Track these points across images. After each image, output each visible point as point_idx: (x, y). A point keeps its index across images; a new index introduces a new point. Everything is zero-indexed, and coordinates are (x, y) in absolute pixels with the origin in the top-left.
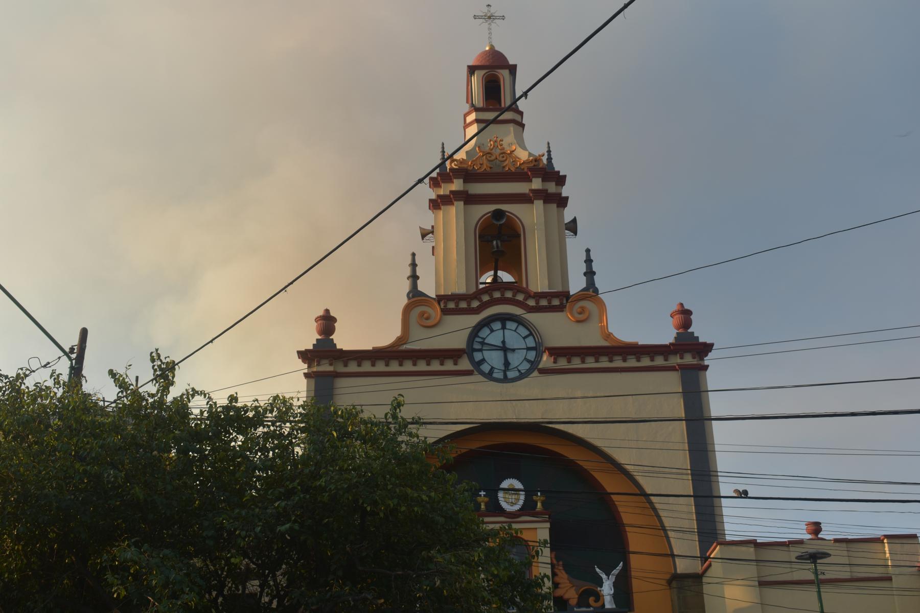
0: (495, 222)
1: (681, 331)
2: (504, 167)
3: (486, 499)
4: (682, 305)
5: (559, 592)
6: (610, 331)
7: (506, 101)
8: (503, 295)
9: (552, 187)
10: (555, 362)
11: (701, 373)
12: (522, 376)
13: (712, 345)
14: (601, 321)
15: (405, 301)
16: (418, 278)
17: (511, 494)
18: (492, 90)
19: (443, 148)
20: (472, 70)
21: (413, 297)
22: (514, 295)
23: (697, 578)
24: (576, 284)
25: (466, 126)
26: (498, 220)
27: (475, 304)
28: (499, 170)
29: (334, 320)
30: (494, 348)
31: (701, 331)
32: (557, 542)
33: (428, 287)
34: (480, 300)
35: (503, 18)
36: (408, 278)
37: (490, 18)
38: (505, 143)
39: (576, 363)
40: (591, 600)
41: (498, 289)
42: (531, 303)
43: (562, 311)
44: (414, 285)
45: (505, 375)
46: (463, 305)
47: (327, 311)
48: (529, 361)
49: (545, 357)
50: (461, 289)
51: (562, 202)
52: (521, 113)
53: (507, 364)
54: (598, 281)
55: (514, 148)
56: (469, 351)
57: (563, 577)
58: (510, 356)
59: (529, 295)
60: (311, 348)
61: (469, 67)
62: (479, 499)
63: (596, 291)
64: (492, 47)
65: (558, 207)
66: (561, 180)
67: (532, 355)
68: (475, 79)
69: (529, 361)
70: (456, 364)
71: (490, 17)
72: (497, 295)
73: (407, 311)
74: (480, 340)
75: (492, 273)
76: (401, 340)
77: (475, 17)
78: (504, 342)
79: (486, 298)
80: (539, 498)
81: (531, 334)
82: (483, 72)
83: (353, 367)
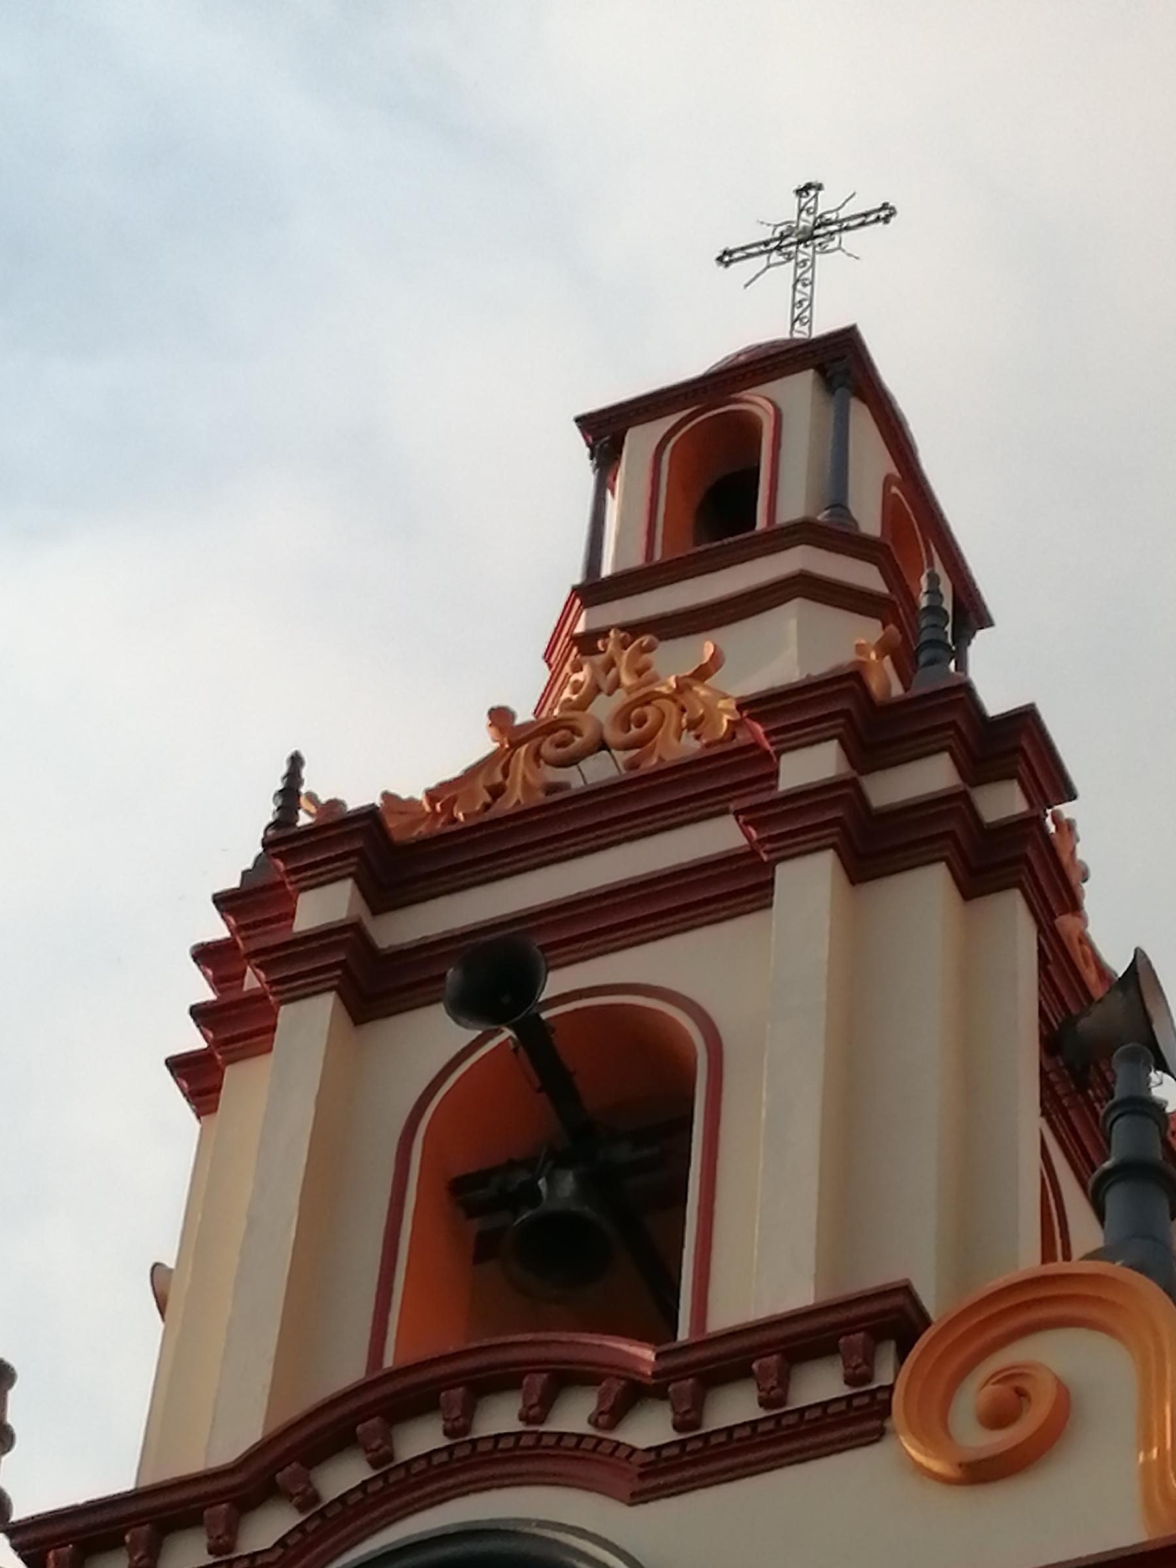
20: (605, 432)
34: (307, 1500)
35: (885, 214)
37: (807, 237)
42: (650, 1429)
43: (877, 1435)
61: (590, 424)
65: (974, 883)
72: (422, 1438)
79: (343, 1476)
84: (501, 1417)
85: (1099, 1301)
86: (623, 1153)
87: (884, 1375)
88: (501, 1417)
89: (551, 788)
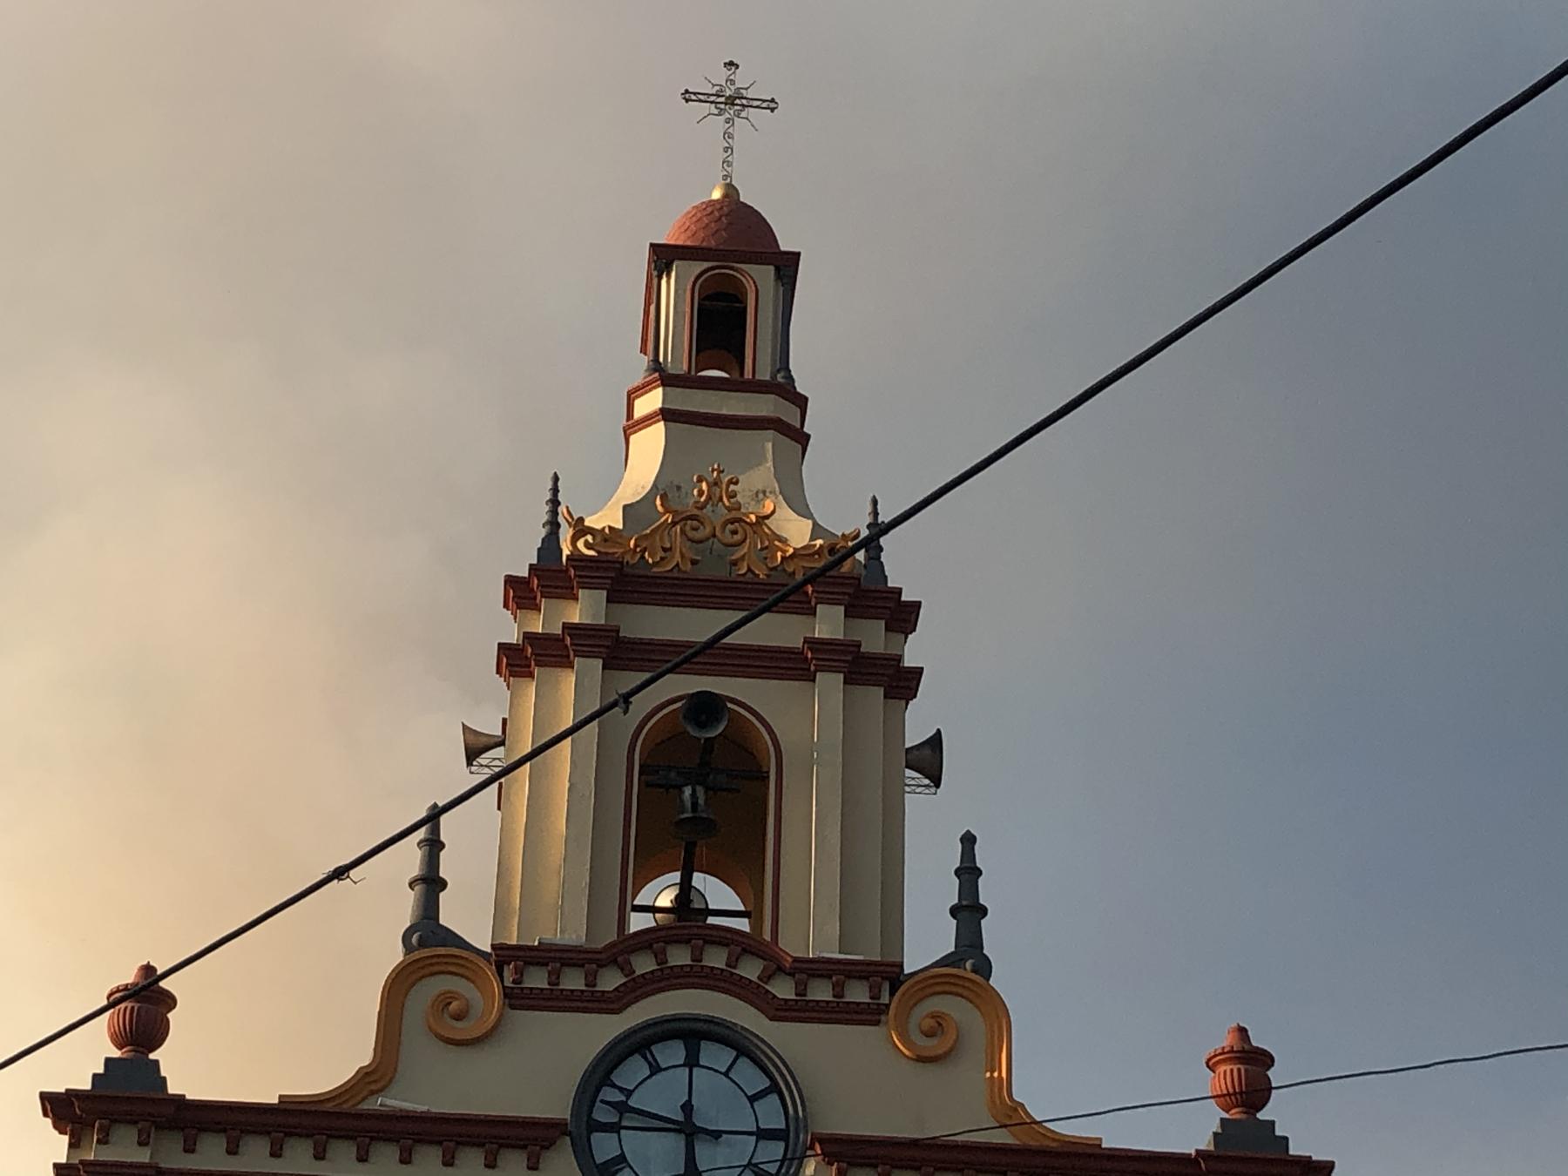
0: (692, 731)
1: (1235, 1114)
2: (734, 563)
4: (1242, 1032)
8: (697, 958)
9: (873, 637)
14: (993, 1065)
15: (397, 955)
16: (443, 884)
18: (720, 325)
19: (555, 490)
20: (663, 257)
21: (422, 944)
22: (733, 962)
24: (926, 940)
25: (633, 426)
26: (702, 726)
27: (611, 981)
28: (721, 572)
29: (169, 1001)
30: (656, 1123)
33: (470, 916)
34: (627, 969)
36: (411, 885)
37: (731, 101)
38: (743, 491)
42: (783, 989)
43: (877, 1023)
46: (573, 981)
50: (574, 934)
51: (904, 684)
52: (801, 402)
55: (769, 506)
56: (579, 1128)
59: (777, 965)
60: (86, 1085)
63: (984, 968)
64: (731, 191)
66: (903, 616)
68: (668, 288)
71: (732, 101)
72: (679, 957)
73: (398, 987)
75: (676, 877)
76: (367, 1080)
77: (687, 96)
78: (687, 1108)
79: (644, 964)
81: (774, 1088)
82: (698, 267)
84: (716, 959)
85: (978, 996)
87: (885, 999)
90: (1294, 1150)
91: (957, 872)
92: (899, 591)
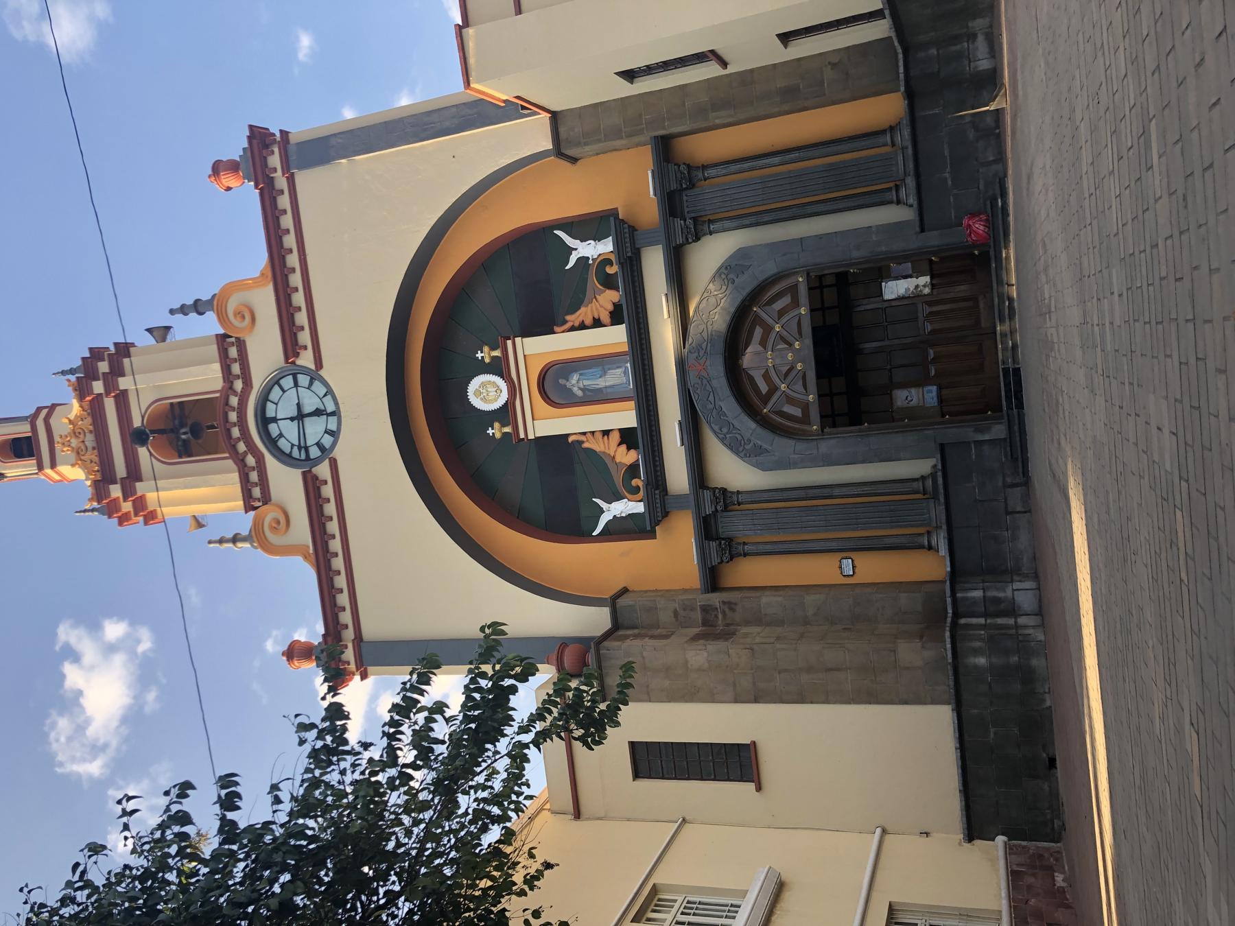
3: (497, 425)
5: (605, 318)
6: (258, 274)
7: (23, 430)
9: (103, 367)
10: (305, 348)
11: (293, 139)
12: (330, 392)
13: (251, 127)
16: (236, 535)
17: (485, 392)
23: (555, 117)
27: (251, 461)
30: (302, 433)
31: (235, 147)
32: (542, 324)
39: (302, 318)
40: (611, 270)
41: (229, 431)
42: (238, 385)
44: (244, 539)
45: (333, 414)
46: (254, 476)
47: (283, 654)
48: (311, 383)
49: (299, 362)
50: (235, 476)
51: (124, 349)
52: (39, 410)
53: (318, 413)
54: (206, 297)
57: (585, 313)
58: (308, 409)
59: (229, 387)
62: (498, 435)
67: (303, 380)
69: (311, 383)
70: (326, 482)
72: (236, 432)
74: (296, 449)
78: (292, 419)
79: (242, 447)
80: (484, 355)
81: (277, 383)
83: (346, 617)
84: (233, 417)
86: (177, 422)
87: (233, 340)
88: (233, 417)
89: (94, 448)
90: (246, 145)
91: (201, 314)
92: (83, 359)
